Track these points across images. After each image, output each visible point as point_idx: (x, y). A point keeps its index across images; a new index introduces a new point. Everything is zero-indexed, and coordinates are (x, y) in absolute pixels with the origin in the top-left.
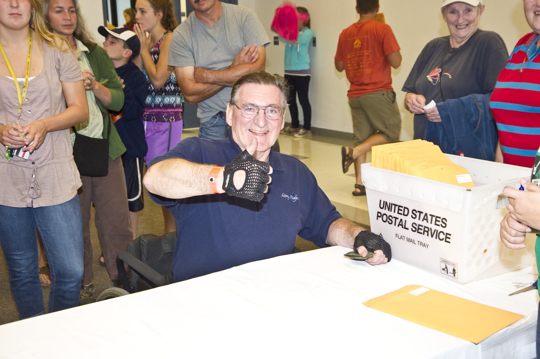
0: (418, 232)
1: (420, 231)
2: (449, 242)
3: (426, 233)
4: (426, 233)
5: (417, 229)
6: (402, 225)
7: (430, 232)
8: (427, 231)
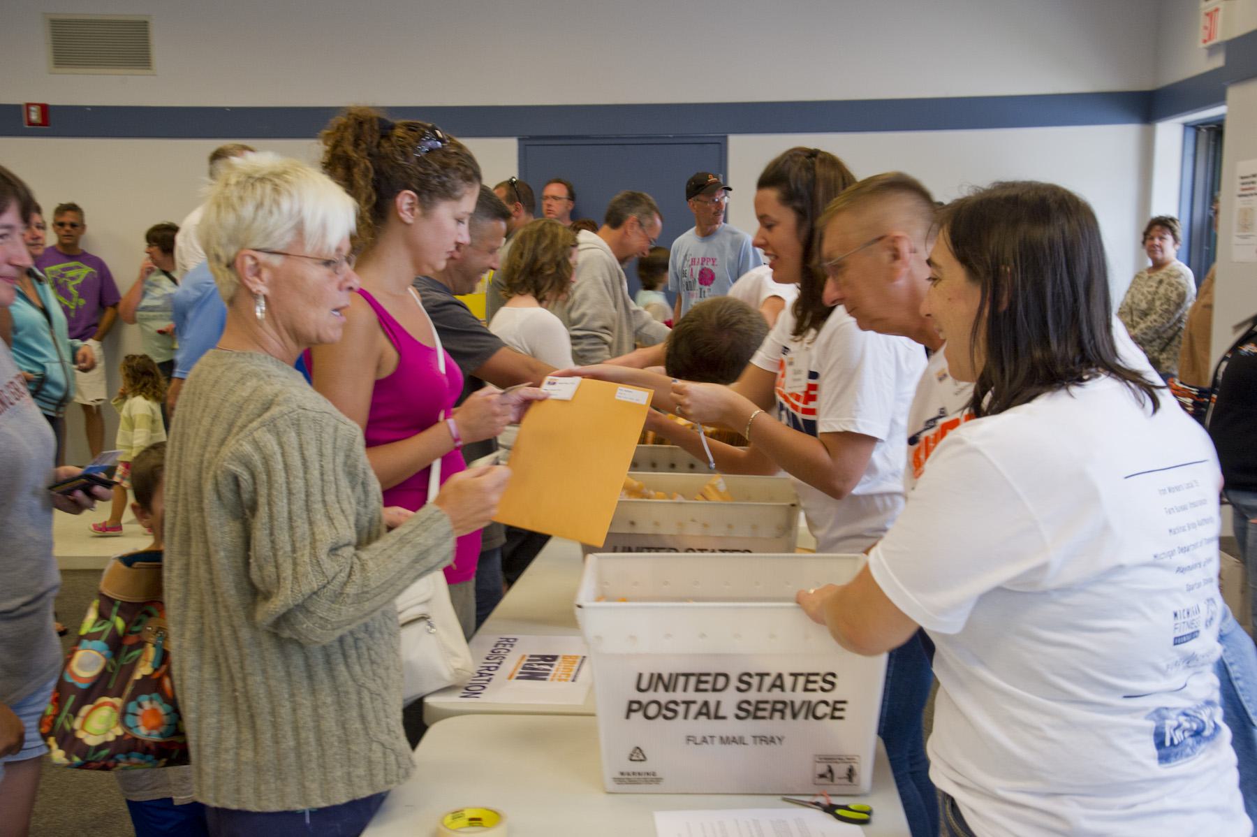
0: (756, 717)
1: (760, 714)
2: (841, 718)
3: (777, 715)
4: (777, 715)
5: (748, 711)
6: (708, 715)
7: (788, 712)
8: (779, 709)
